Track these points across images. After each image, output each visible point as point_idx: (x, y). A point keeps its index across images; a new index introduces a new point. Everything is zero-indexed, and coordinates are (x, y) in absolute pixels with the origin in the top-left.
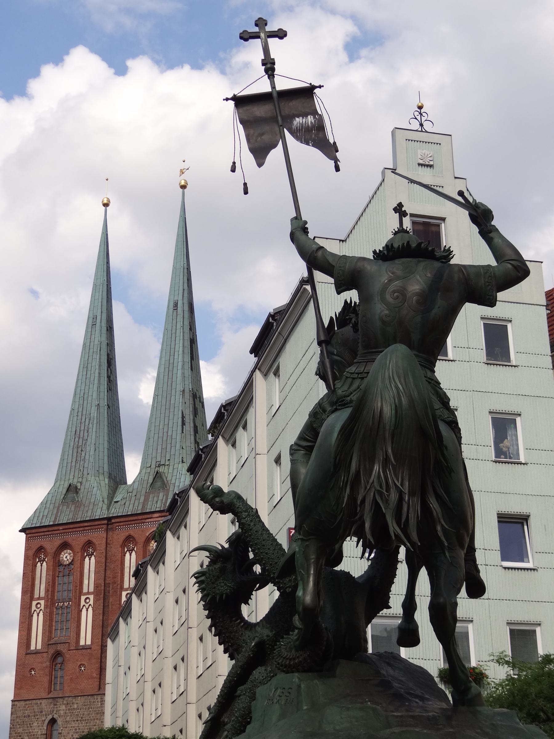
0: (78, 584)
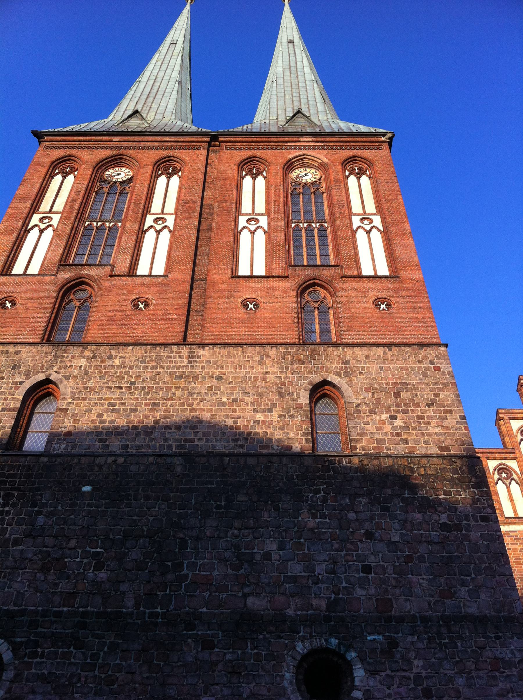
0: (144, 197)
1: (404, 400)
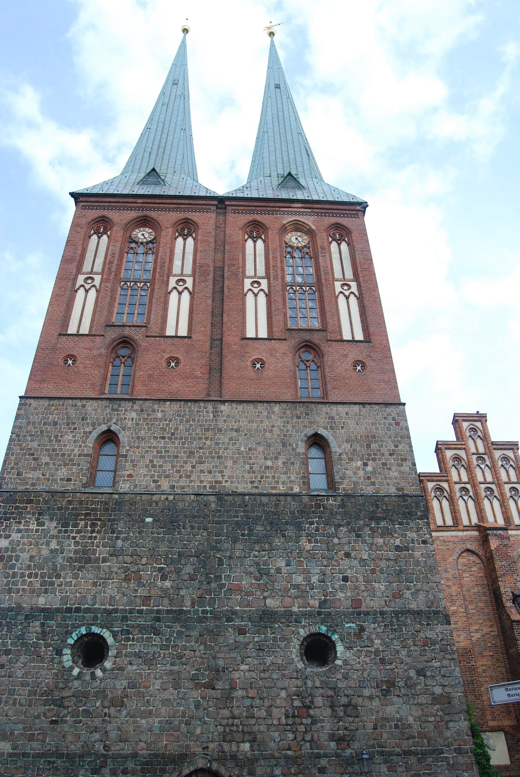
0: (167, 260)
1: (373, 450)
